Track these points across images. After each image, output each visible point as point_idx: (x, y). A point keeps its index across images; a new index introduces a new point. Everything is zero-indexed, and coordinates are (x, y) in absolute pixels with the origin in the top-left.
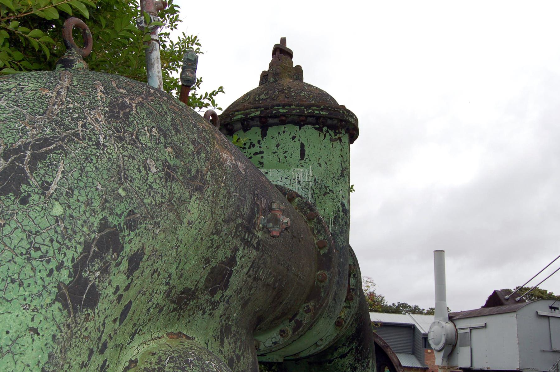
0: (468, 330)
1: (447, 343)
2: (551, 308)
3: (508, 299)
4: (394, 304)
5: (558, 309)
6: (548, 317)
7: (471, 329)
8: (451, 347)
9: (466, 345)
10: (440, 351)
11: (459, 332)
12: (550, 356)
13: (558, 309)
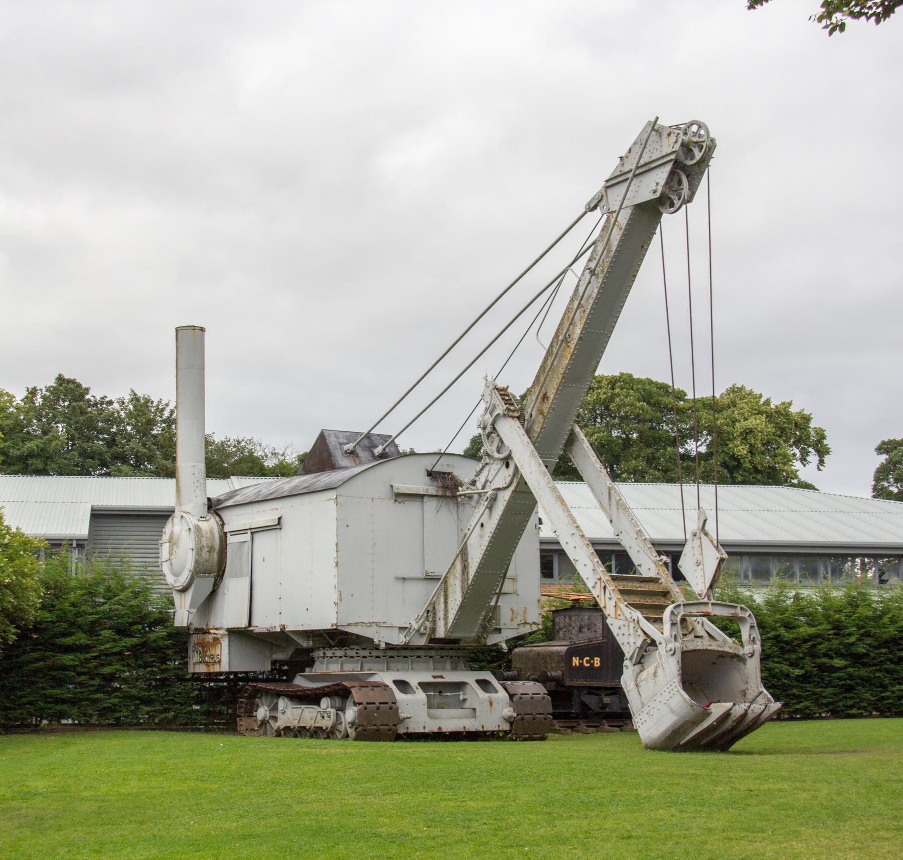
0: (247, 537)
6: (421, 496)
7: (254, 531)
10: (184, 590)
11: (231, 539)
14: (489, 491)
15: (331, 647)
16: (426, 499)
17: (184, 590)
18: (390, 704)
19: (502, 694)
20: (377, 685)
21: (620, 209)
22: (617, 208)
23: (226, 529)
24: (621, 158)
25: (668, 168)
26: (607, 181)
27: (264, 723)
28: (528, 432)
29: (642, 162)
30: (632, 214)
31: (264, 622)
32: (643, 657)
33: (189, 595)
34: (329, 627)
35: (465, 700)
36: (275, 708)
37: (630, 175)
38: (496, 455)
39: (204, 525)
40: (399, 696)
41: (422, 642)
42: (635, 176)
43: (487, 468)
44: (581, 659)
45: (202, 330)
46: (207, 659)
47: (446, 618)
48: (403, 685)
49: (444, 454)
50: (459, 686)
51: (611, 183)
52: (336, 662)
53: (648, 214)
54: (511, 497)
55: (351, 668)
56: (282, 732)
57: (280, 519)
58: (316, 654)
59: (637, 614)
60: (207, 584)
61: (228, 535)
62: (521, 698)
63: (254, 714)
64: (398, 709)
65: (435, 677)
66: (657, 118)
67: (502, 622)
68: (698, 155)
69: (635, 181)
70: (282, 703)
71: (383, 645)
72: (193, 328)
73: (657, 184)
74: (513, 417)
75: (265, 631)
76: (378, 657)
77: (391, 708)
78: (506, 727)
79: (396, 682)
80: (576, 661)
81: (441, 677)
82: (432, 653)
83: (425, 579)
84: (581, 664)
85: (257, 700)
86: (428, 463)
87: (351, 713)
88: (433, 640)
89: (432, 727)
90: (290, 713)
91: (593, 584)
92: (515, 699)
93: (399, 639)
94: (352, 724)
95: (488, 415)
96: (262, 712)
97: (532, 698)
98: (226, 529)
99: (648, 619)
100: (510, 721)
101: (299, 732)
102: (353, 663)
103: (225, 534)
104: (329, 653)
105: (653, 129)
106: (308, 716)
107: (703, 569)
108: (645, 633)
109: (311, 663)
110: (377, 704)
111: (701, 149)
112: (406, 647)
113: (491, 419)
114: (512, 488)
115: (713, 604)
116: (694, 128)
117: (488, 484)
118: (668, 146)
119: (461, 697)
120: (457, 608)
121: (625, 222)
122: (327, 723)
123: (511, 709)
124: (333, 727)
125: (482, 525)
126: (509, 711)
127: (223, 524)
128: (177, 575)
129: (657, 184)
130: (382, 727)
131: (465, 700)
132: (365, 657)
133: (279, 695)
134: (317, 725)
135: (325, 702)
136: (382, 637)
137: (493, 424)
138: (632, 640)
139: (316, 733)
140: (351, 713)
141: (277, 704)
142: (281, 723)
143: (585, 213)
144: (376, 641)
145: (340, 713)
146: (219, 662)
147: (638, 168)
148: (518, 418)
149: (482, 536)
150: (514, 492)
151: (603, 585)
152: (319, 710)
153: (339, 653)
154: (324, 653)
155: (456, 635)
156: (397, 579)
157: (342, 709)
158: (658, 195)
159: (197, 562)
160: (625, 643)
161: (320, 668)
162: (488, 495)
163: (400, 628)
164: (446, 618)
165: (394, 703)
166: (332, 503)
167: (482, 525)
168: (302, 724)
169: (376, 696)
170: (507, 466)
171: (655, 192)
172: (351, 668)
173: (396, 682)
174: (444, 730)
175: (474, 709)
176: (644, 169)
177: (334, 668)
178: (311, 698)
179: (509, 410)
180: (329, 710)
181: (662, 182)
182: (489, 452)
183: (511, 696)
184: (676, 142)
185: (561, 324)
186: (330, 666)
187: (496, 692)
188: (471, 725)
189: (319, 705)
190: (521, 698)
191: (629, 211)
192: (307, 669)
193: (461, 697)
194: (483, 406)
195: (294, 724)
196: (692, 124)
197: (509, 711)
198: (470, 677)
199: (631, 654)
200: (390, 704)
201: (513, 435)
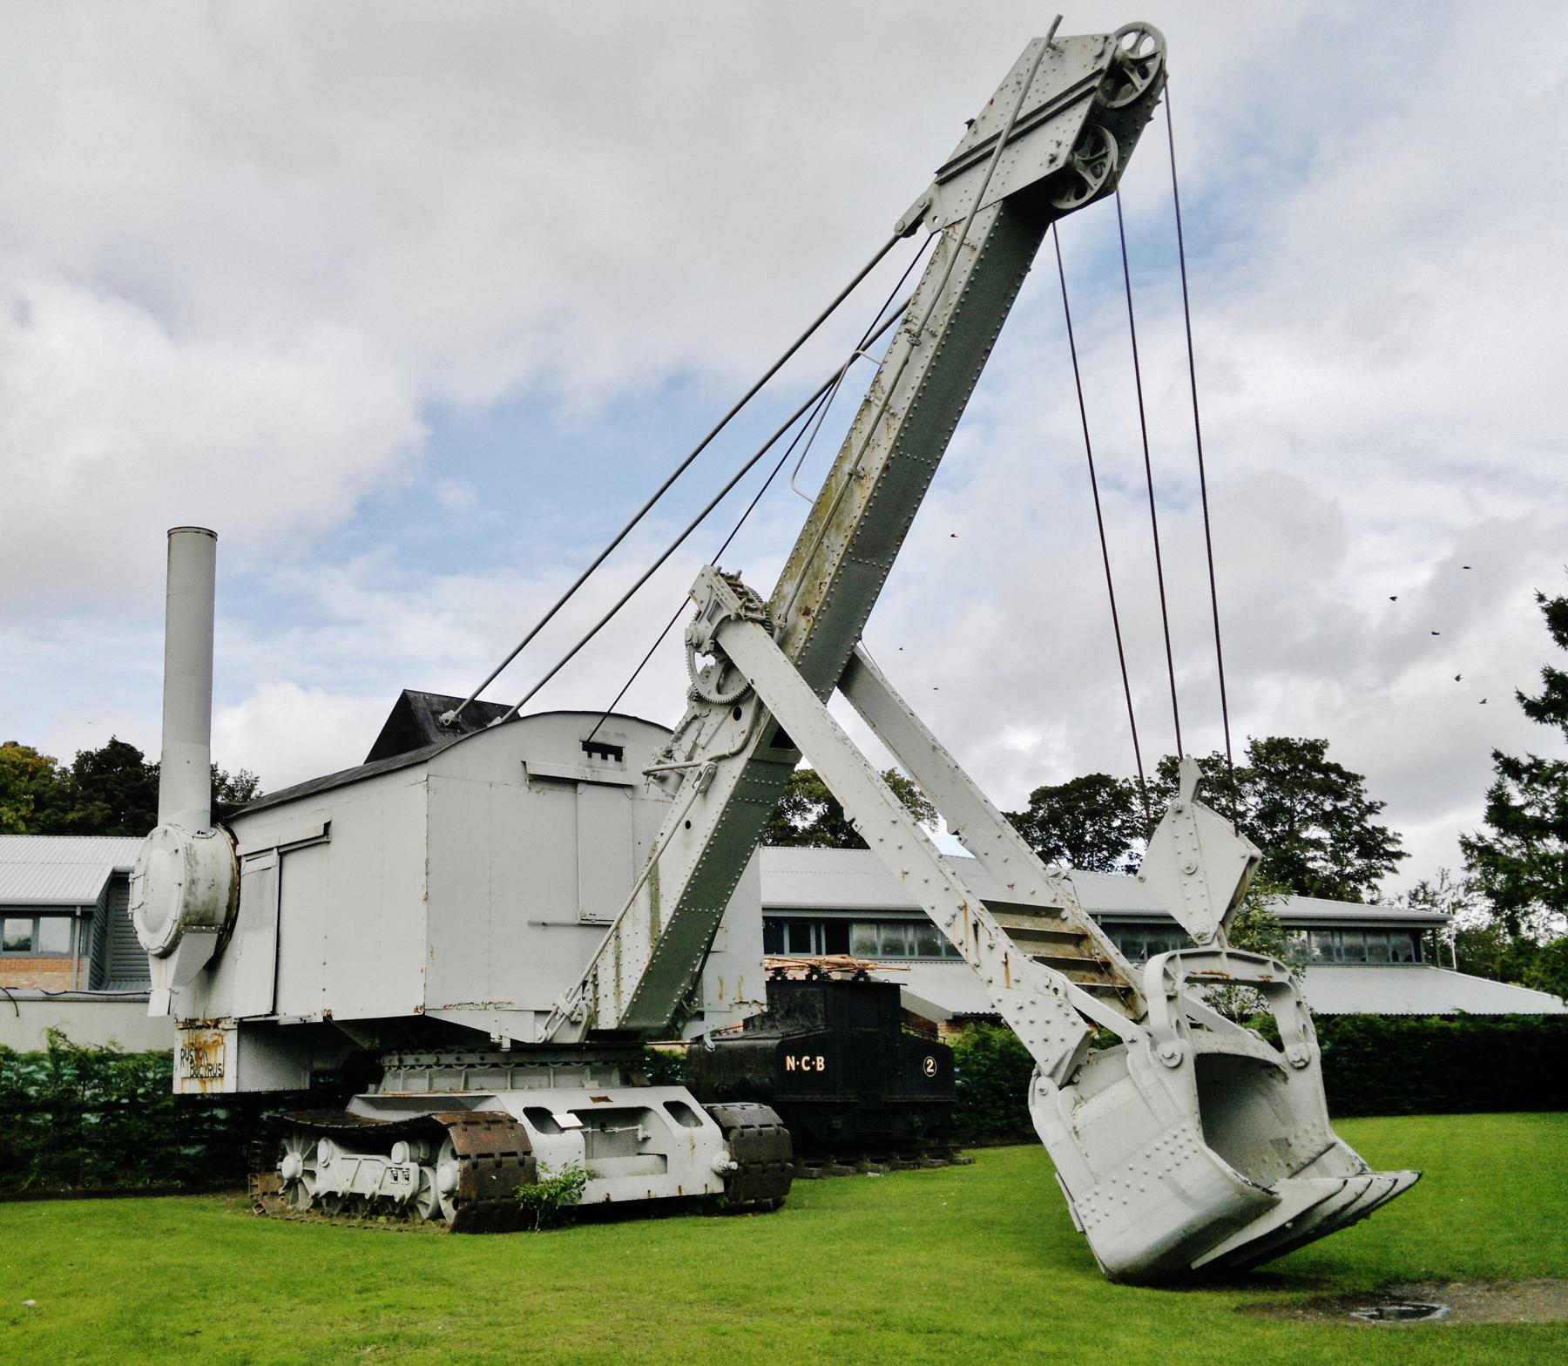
0: (273, 858)
1: (194, 921)
2: (590, 747)
6: (573, 783)
7: (284, 852)
10: (165, 954)
11: (247, 867)
14: (703, 760)
16: (581, 787)
17: (165, 954)
18: (520, 1156)
19: (711, 1129)
20: (494, 1121)
21: (976, 211)
22: (968, 214)
23: (240, 851)
24: (970, 123)
26: (940, 172)
27: (293, 1183)
28: (782, 644)
30: (999, 218)
32: (1077, 1070)
33: (175, 959)
35: (646, 1139)
36: (312, 1156)
37: (999, 143)
38: (715, 697)
39: (201, 846)
40: (535, 1137)
41: (574, 1036)
42: (1009, 142)
43: (696, 725)
46: (202, 1071)
47: (618, 994)
48: (540, 1117)
51: (948, 175)
52: (422, 1075)
53: (1029, 215)
54: (746, 770)
55: (448, 1086)
56: (324, 1202)
57: (327, 825)
58: (386, 1061)
59: (1059, 978)
60: (205, 945)
62: (742, 1134)
64: (534, 1164)
65: (595, 1100)
66: (1059, 19)
67: (706, 1000)
68: (1141, 84)
69: (1006, 155)
70: (325, 1148)
71: (506, 1045)
72: (198, 530)
73: (1059, 144)
74: (754, 620)
75: (297, 1021)
76: (495, 1065)
77: (522, 1163)
78: (718, 1187)
79: (529, 1112)
81: (606, 1099)
82: (590, 1058)
85: (284, 1142)
86: (584, 728)
88: (592, 1034)
90: (338, 1170)
91: (948, 919)
92: (734, 1134)
93: (534, 1033)
94: (449, 1194)
96: (291, 1164)
97: (760, 1133)
98: (240, 851)
99: (1091, 990)
101: (348, 1204)
102: (449, 1075)
103: (239, 859)
104: (410, 1060)
105: (1049, 45)
110: (497, 1157)
111: (1144, 75)
114: (748, 754)
115: (1230, 955)
116: (1128, 41)
117: (699, 751)
120: (640, 975)
121: (984, 235)
122: (401, 1190)
123: (727, 1155)
124: (414, 1197)
125: (688, 825)
127: (236, 842)
128: (153, 929)
129: (1059, 144)
130: (505, 1202)
131: (646, 1139)
132: (471, 1066)
133: (320, 1134)
136: (506, 1029)
137: (715, 636)
139: (381, 1206)
141: (316, 1148)
142: (321, 1186)
143: (896, 239)
144: (495, 1037)
145: (425, 1169)
147: (1016, 125)
148: (762, 623)
149: (688, 845)
150: (750, 760)
151: (972, 920)
152: (389, 1163)
154: (400, 1060)
155: (634, 1024)
156: (532, 924)
157: (430, 1162)
158: (1060, 163)
159: (186, 906)
161: (392, 1086)
162: (702, 769)
163: (537, 1013)
164: (618, 994)
165: (528, 1153)
166: (420, 790)
167: (688, 825)
169: (495, 1141)
170: (737, 716)
172: (448, 1086)
173: (529, 1112)
174: (614, 1199)
175: (664, 1157)
176: (1023, 129)
177: (418, 1087)
178: (374, 1141)
179: (747, 608)
181: (1070, 138)
182: (704, 694)
183: (726, 1132)
184: (1100, 56)
186: (410, 1083)
187: (699, 1123)
188: (663, 1188)
189: (388, 1154)
190: (742, 1134)
191: (993, 213)
192: (372, 1087)
193: (640, 1136)
194: (693, 608)
195: (342, 1188)
196: (1123, 33)
198: (653, 1098)
199: (1052, 1063)
200: (520, 1156)
201: (755, 653)
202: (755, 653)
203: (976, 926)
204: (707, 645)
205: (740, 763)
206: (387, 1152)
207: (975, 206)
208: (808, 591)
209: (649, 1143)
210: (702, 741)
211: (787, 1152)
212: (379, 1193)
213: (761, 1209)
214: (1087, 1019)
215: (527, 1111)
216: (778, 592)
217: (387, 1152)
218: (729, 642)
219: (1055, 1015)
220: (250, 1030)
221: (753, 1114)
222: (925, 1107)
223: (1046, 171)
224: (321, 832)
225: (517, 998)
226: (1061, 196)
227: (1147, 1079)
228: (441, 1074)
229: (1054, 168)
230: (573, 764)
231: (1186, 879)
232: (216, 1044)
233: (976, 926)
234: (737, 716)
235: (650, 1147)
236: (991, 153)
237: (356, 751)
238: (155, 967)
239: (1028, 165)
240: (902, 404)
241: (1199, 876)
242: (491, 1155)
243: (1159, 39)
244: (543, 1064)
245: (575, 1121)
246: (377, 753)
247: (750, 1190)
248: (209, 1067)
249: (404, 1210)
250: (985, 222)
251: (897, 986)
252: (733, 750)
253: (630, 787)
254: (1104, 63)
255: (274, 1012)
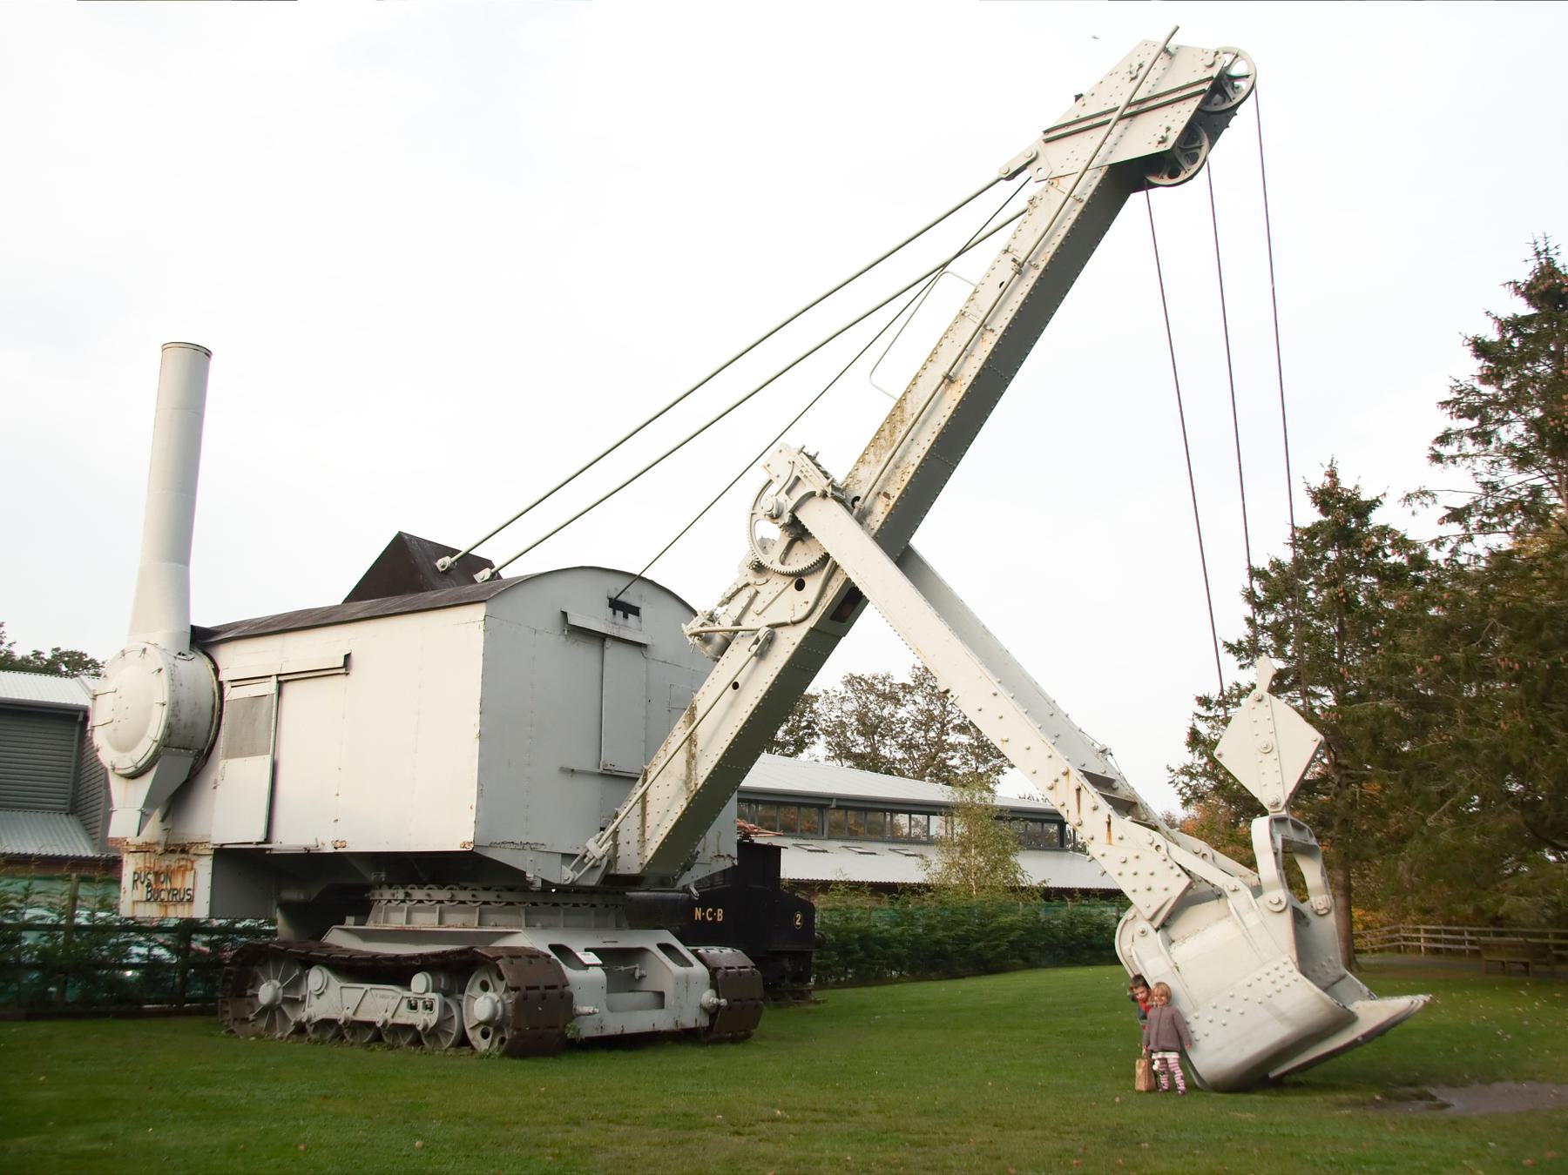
0: (270, 687)
1: (172, 741)
2: (616, 605)
3: (448, 572)
4: (37, 654)
5: (636, 611)
6: (601, 638)
8: (187, 756)
9: (253, 752)
11: (231, 694)
12: (589, 791)
13: (636, 611)
15: (421, 884)
19: (699, 969)
25: (1193, 104)
26: (1046, 132)
27: (272, 1009)
29: (1138, 97)
30: (1103, 180)
31: (292, 837)
33: (148, 780)
34: (457, 848)
35: (642, 977)
40: (570, 973)
41: (593, 880)
42: (1122, 118)
44: (704, 911)
45: (208, 354)
49: (640, 578)
50: (642, 951)
51: (1054, 136)
52: (430, 910)
54: (806, 639)
57: (347, 657)
61: (227, 687)
63: (249, 992)
71: (539, 884)
73: (1168, 129)
76: (509, 904)
77: (562, 996)
80: (698, 913)
83: (601, 774)
84: (704, 917)
86: (614, 587)
87: (482, 1005)
89: (615, 1024)
90: (329, 998)
93: (567, 875)
95: (783, 497)
96: (266, 992)
98: (221, 678)
100: (712, 1012)
102: (461, 912)
104: (418, 894)
106: (380, 1004)
107: (1278, 759)
108: (1188, 873)
109: (363, 909)
112: (570, 891)
113: (791, 505)
114: (811, 622)
118: (1192, 72)
119: (637, 974)
121: (1090, 191)
122: (422, 1019)
126: (709, 997)
127: (216, 671)
128: (124, 748)
129: (1168, 129)
130: (542, 1028)
131: (642, 977)
133: (308, 964)
134: (398, 1020)
135: (420, 982)
136: (537, 870)
137: (793, 512)
138: (1157, 883)
140: (482, 1005)
142: (316, 1009)
144: (529, 875)
145: (448, 1001)
146: (191, 901)
147: (1129, 105)
152: (407, 994)
153: (443, 894)
154: (407, 894)
159: (169, 726)
160: (1141, 889)
163: (564, 855)
164: (643, 841)
167: (736, 686)
168: (362, 1017)
170: (800, 586)
171: (1163, 140)
172: (461, 921)
175: (661, 995)
176: (1136, 110)
177: (426, 920)
178: (395, 972)
180: (434, 996)
181: (1179, 126)
183: (714, 971)
185: (935, 352)
192: (350, 921)
197: (709, 997)
198: (649, 940)
201: (833, 529)
202: (833, 529)
203: (1079, 790)
204: (786, 518)
205: (803, 630)
206: (405, 982)
207: (1080, 165)
208: (888, 479)
209: (645, 981)
210: (758, 605)
211: (759, 991)
212: (391, 1021)
213: (734, 1040)
214: (1188, 873)
215: (552, 947)
216: (850, 475)
217: (405, 982)
218: (806, 517)
219: (1161, 869)
220: (226, 857)
221: (725, 955)
222: (792, 955)
223: (1153, 149)
224: (341, 664)
225: (558, 837)
226: (1156, 173)
227: (1252, 919)
228: (453, 910)
229: (1162, 148)
230: (598, 619)
231: (1261, 757)
232: (183, 870)
233: (1079, 790)
234: (800, 586)
235: (646, 985)
236: (1107, 122)
237: (334, 592)
238: (117, 787)
239: (1143, 139)
240: (1001, 323)
241: (1274, 755)
242: (537, 988)
243: (1250, 63)
244: (555, 905)
245: (596, 960)
246: (358, 594)
247: (724, 1028)
248: (173, 892)
249: (443, 1038)
250: (1093, 180)
251: (778, 849)
252: (796, 618)
253: (641, 646)
254: (1214, 72)
255: (268, 840)
